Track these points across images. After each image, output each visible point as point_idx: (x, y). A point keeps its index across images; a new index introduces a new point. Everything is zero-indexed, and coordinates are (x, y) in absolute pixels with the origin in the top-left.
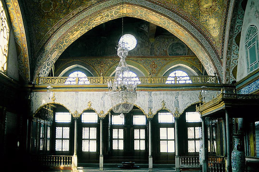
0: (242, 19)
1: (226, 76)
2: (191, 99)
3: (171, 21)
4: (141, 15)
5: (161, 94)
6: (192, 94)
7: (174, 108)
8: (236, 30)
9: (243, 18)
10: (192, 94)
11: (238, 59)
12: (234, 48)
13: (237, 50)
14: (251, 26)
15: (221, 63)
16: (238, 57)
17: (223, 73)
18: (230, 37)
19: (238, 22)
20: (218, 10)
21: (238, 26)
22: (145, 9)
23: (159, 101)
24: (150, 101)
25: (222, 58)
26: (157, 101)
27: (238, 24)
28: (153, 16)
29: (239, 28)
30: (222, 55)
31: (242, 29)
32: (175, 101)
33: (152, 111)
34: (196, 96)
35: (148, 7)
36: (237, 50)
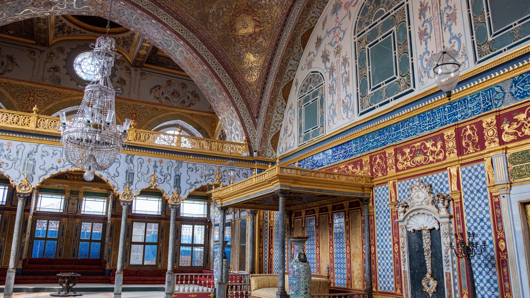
0: (298, 61)
2: (202, 177)
3: (182, 42)
4: (128, 20)
9: (300, 59)
12: (278, 104)
13: (283, 108)
14: (312, 72)
15: (256, 125)
16: (283, 117)
17: (256, 140)
18: (277, 84)
19: (291, 65)
20: (262, 42)
21: (290, 70)
22: (139, 11)
25: (257, 117)
27: (290, 68)
28: (151, 28)
29: (291, 74)
30: (258, 112)
35: (145, 8)
36: (283, 108)
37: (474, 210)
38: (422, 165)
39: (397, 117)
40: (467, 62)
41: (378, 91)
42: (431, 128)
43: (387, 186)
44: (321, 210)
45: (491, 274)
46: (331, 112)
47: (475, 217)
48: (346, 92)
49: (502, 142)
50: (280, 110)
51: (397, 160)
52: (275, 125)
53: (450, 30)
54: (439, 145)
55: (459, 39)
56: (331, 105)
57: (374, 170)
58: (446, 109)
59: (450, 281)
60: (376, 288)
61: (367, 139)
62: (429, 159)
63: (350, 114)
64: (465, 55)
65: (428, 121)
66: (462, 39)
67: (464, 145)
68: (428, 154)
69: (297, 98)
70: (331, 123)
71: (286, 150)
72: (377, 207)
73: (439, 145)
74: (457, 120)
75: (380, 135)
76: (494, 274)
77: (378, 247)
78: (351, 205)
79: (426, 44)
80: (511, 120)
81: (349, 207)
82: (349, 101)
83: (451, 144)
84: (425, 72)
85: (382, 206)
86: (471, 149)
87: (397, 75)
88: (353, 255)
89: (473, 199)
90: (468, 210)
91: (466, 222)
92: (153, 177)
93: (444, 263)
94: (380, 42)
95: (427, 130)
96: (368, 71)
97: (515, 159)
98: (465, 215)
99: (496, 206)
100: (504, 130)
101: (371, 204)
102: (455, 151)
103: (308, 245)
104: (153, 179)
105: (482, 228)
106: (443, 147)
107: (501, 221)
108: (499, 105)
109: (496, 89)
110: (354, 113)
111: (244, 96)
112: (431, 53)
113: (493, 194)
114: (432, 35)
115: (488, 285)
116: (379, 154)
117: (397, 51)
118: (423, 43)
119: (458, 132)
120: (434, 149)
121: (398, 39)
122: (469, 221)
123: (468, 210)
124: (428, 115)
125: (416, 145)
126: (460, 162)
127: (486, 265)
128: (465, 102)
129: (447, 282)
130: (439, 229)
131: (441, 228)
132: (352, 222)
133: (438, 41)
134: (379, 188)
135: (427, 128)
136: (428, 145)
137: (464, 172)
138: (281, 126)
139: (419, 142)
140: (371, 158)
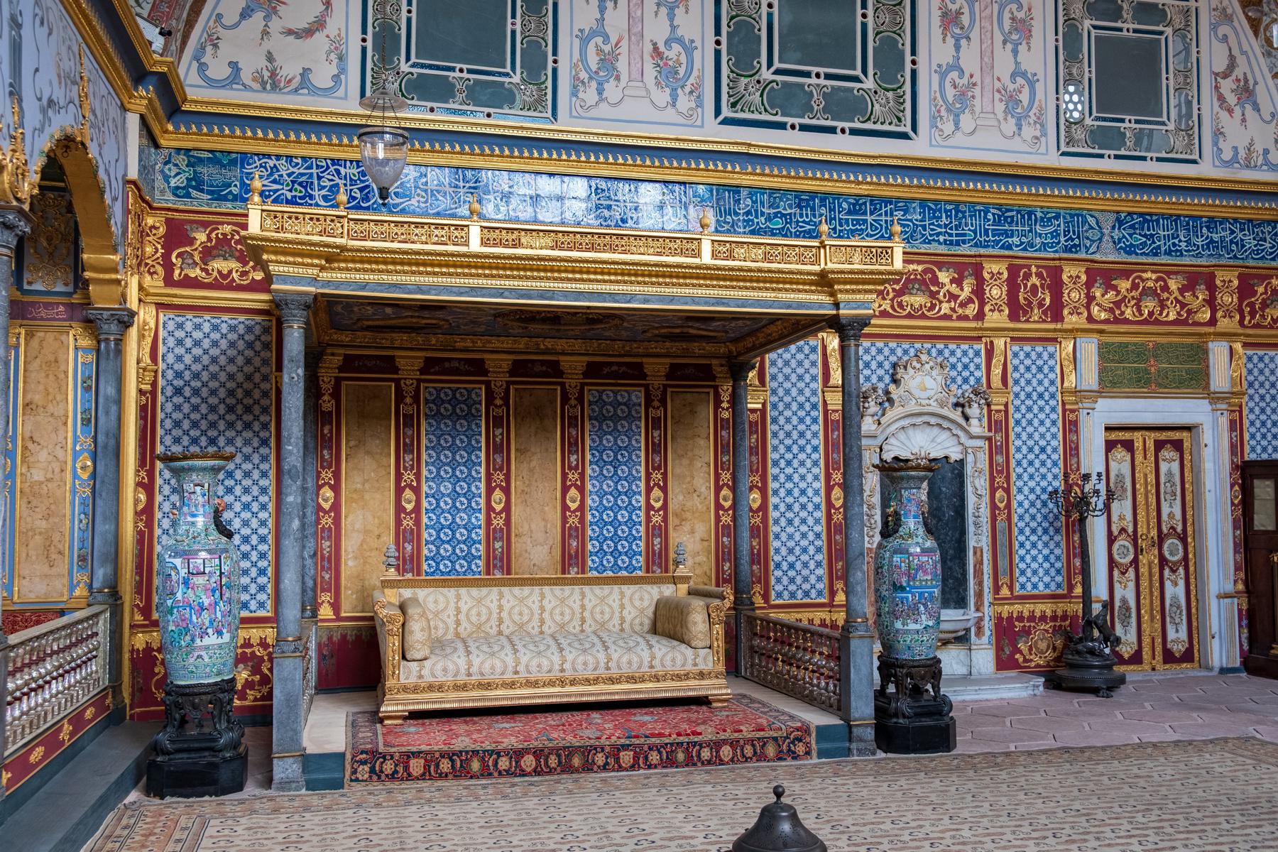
37: (1030, 429)
38: (923, 317)
39: (871, 183)
40: (1043, 139)
41: (801, 86)
42: (951, 243)
44: (519, 368)
45: (1052, 545)
46: (593, 60)
47: (1030, 443)
48: (673, 28)
49: (1090, 319)
53: (1015, 52)
55: (1032, 84)
56: (593, 33)
58: (990, 216)
59: (981, 563)
60: (766, 597)
61: (749, 202)
63: (684, 102)
64: (1042, 125)
65: (946, 226)
66: (1039, 87)
67: (1022, 301)
70: (590, 95)
71: (272, 81)
72: (774, 392)
74: (1009, 247)
75: (799, 206)
76: (1058, 545)
77: (776, 492)
78: (675, 372)
79: (957, 47)
80: (1109, 287)
81: (668, 377)
82: (683, 59)
83: (996, 292)
84: (949, 110)
85: (794, 392)
86: (1036, 314)
88: (677, 515)
89: (1029, 409)
90: (1018, 429)
91: (1012, 450)
95: (940, 243)
97: (1109, 352)
98: (1012, 436)
99: (1071, 426)
100: (1094, 298)
102: (1007, 312)
105: (1043, 464)
106: (979, 292)
107: (1078, 455)
108: (1091, 251)
109: (1090, 219)
110: (700, 105)
112: (967, 75)
113: (1068, 407)
114: (975, 35)
115: (1046, 565)
117: (870, 12)
118: (951, 41)
119: (1013, 271)
120: (954, 289)
122: (1018, 450)
123: (1018, 429)
124: (946, 211)
127: (1045, 531)
128: (1030, 219)
131: (970, 458)
132: (677, 422)
133: (986, 59)
135: (941, 238)
136: (944, 277)
137: (1016, 355)
139: (919, 263)
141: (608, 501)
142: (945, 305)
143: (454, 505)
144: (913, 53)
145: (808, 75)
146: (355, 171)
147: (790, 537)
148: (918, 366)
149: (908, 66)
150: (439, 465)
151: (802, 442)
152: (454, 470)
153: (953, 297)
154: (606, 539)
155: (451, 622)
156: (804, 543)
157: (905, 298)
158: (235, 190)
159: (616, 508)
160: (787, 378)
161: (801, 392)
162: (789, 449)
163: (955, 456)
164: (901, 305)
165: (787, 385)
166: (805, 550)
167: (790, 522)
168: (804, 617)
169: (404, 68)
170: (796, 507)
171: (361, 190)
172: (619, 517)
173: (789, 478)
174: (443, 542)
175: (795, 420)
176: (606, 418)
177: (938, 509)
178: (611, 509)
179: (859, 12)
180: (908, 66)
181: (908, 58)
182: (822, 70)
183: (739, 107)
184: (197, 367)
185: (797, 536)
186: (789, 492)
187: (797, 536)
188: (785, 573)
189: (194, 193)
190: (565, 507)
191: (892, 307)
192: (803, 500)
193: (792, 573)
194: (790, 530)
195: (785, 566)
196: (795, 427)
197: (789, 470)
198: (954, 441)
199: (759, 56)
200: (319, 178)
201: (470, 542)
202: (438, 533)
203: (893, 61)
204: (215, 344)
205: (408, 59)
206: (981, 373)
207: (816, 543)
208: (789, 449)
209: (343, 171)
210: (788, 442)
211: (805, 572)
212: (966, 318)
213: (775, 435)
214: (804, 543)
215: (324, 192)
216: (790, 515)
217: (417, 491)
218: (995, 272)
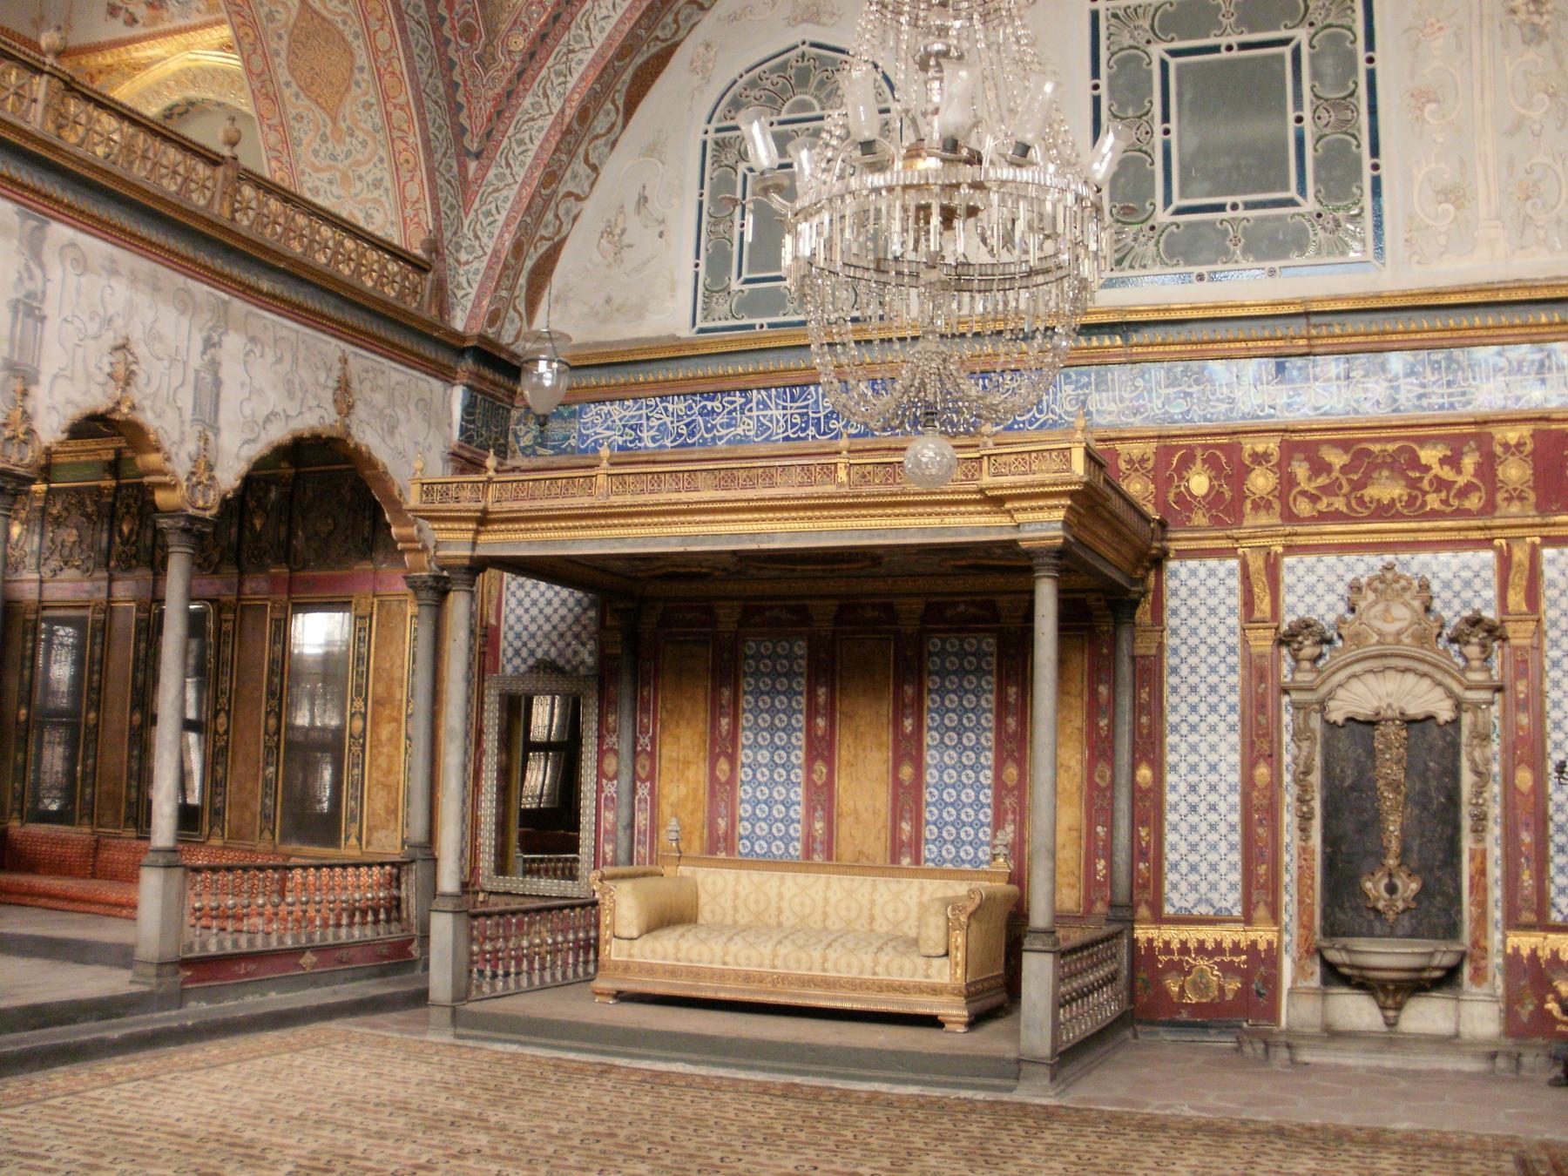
1: (496, 289)
2: (291, 394)
5: (114, 272)
6: (302, 353)
7: (187, 427)
8: (670, 18)
10: (302, 353)
11: (588, 207)
12: (601, 124)
16: (593, 184)
23: (93, 328)
24: (29, 309)
25: (478, 156)
26: (78, 324)
31: (697, 28)
32: (197, 372)
33: (30, 410)
34: (322, 377)
38: (1399, 517)
41: (1212, 224)
43: (1234, 563)
50: (595, 148)
51: (1287, 483)
52: (561, 212)
54: (1469, 462)
57: (1171, 497)
62: (1424, 504)
68: (1425, 485)
69: (703, 126)
73: (1469, 462)
77: (1174, 768)
85: (1203, 631)
87: (1302, 190)
92: (119, 355)
93: (1466, 823)
94: (1224, 55)
96: (1158, 138)
101: (1143, 614)
102: (1532, 496)
103: (755, 746)
104: (121, 370)
111: (447, 42)
116: (1206, 447)
120: (1447, 473)
121: (1316, 75)
125: (1376, 448)
126: (1546, 531)
129: (1472, 878)
130: (1455, 723)
131: (1467, 719)
134: (1193, 564)
136: (1429, 455)
138: (575, 219)
140: (1165, 453)
141: (950, 776)
142: (1429, 498)
143: (772, 778)
144: (1375, 151)
145: (1220, 208)
146: (682, 406)
147: (1193, 828)
148: (1381, 587)
149: (1367, 173)
150: (757, 730)
151: (1213, 699)
152: (772, 736)
153: (1441, 484)
154: (946, 824)
155: (728, 906)
156: (1213, 837)
157: (1371, 492)
158: (573, 442)
159: (959, 786)
160: (1193, 612)
161: (1213, 631)
162: (1194, 709)
163: (1445, 713)
164: (1361, 501)
165: (1193, 622)
166: (1213, 847)
167: (1193, 808)
168: (1209, 935)
169: (735, 285)
170: (1203, 788)
171: (687, 425)
172: (963, 797)
173: (1193, 748)
174: (759, 819)
175: (1203, 670)
176: (949, 673)
177: (1424, 793)
178: (953, 786)
179: (1291, 116)
180: (1367, 173)
181: (1367, 161)
182: (1239, 199)
183: (1126, 264)
184: (533, 628)
185: (1203, 828)
186: (1193, 768)
187: (1203, 828)
188: (1184, 877)
189: (541, 451)
190: (897, 783)
191: (1348, 505)
192: (1213, 778)
193: (1194, 878)
194: (1193, 819)
195: (1184, 867)
196: (1203, 679)
197: (1194, 738)
198: (1439, 691)
199: (1152, 194)
200: (648, 418)
201: (788, 821)
202: (754, 808)
203: (1348, 170)
204: (549, 603)
205: (740, 275)
206: (1490, 594)
207: (1230, 837)
208: (1194, 709)
209: (670, 407)
210: (1193, 699)
211: (1213, 877)
212: (1467, 514)
213: (1175, 690)
214: (1213, 837)
215: (653, 433)
216: (1193, 798)
217: (732, 759)
218: (1513, 442)
